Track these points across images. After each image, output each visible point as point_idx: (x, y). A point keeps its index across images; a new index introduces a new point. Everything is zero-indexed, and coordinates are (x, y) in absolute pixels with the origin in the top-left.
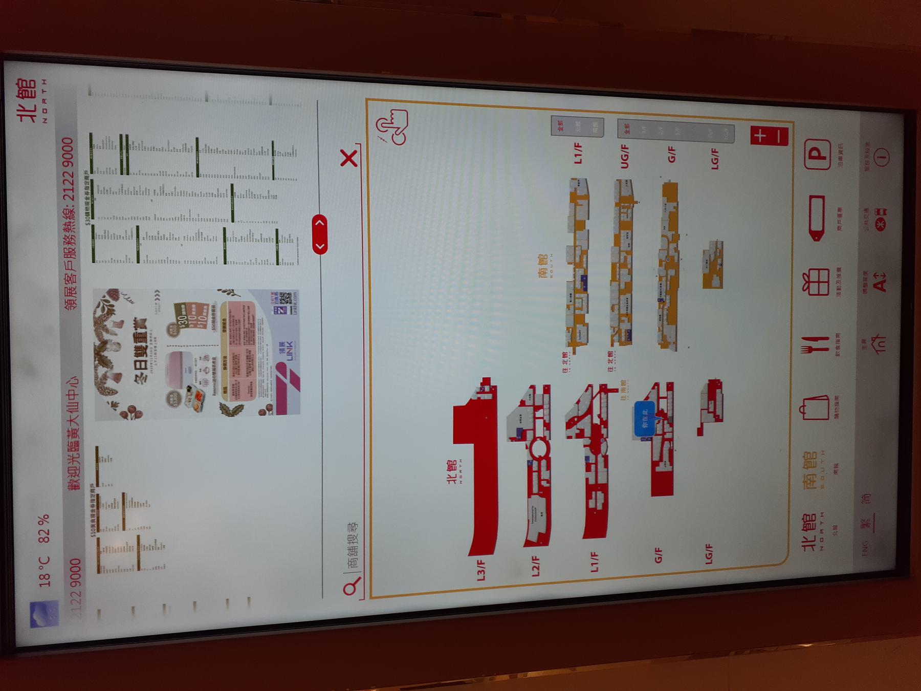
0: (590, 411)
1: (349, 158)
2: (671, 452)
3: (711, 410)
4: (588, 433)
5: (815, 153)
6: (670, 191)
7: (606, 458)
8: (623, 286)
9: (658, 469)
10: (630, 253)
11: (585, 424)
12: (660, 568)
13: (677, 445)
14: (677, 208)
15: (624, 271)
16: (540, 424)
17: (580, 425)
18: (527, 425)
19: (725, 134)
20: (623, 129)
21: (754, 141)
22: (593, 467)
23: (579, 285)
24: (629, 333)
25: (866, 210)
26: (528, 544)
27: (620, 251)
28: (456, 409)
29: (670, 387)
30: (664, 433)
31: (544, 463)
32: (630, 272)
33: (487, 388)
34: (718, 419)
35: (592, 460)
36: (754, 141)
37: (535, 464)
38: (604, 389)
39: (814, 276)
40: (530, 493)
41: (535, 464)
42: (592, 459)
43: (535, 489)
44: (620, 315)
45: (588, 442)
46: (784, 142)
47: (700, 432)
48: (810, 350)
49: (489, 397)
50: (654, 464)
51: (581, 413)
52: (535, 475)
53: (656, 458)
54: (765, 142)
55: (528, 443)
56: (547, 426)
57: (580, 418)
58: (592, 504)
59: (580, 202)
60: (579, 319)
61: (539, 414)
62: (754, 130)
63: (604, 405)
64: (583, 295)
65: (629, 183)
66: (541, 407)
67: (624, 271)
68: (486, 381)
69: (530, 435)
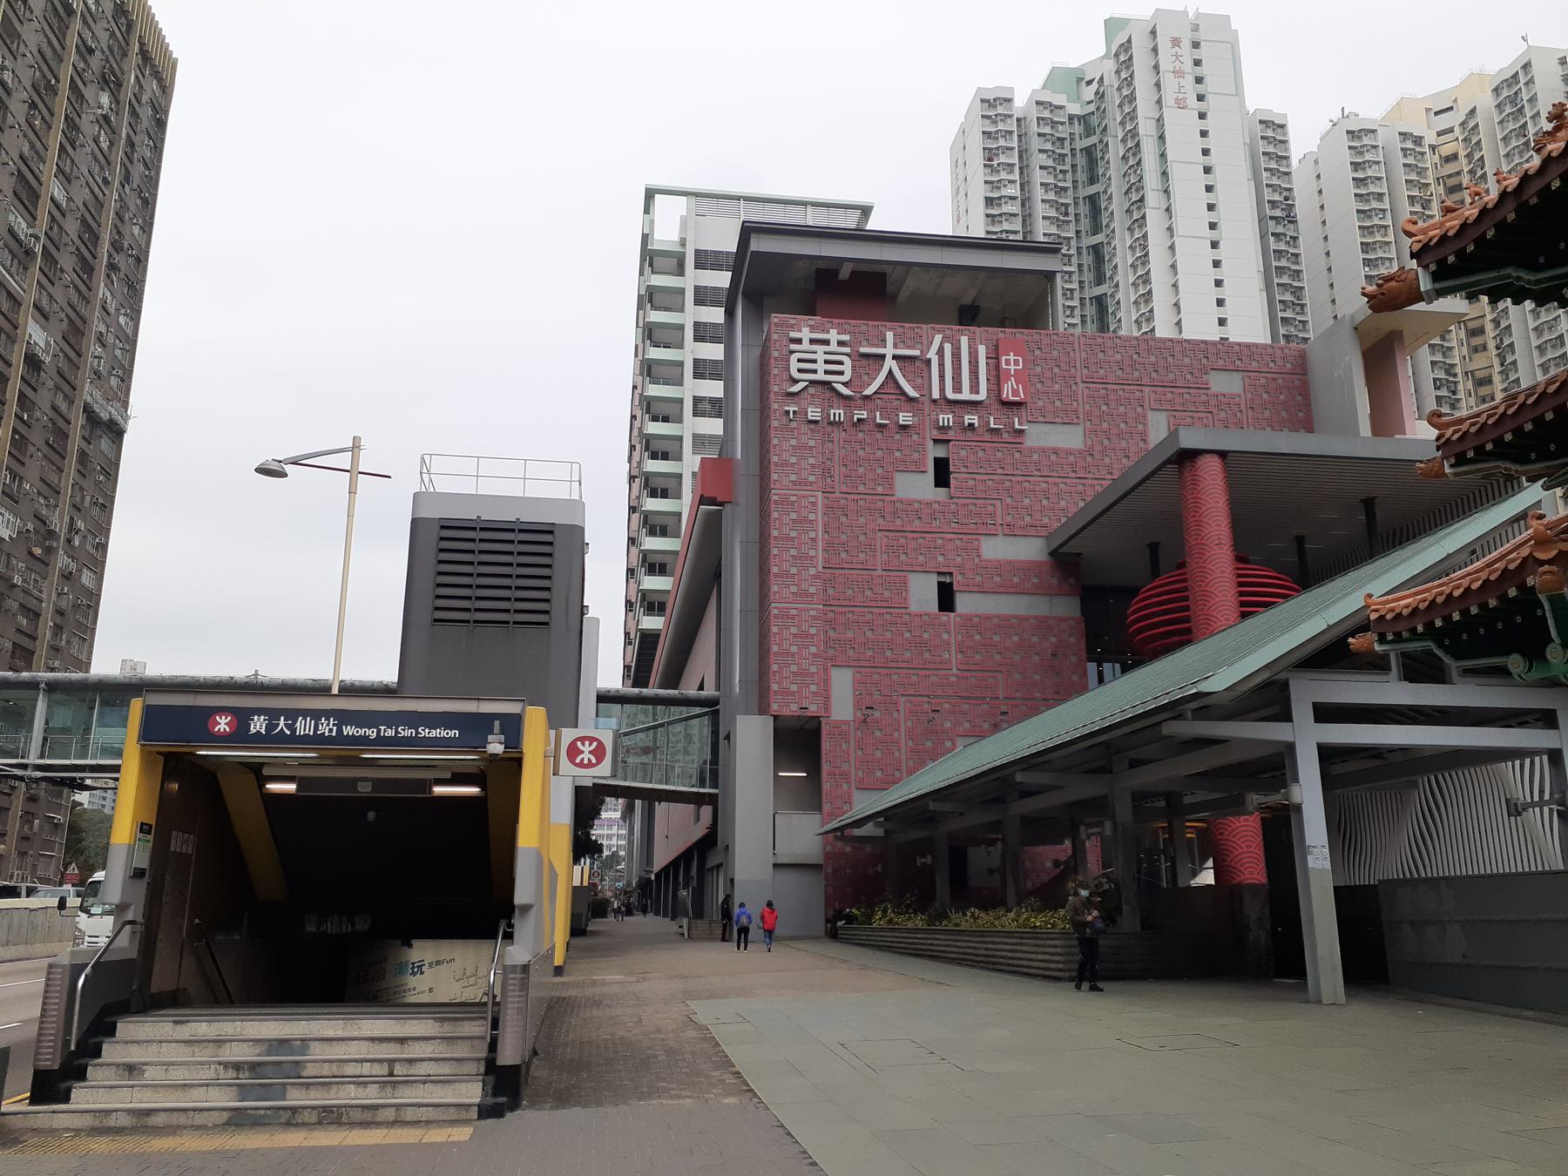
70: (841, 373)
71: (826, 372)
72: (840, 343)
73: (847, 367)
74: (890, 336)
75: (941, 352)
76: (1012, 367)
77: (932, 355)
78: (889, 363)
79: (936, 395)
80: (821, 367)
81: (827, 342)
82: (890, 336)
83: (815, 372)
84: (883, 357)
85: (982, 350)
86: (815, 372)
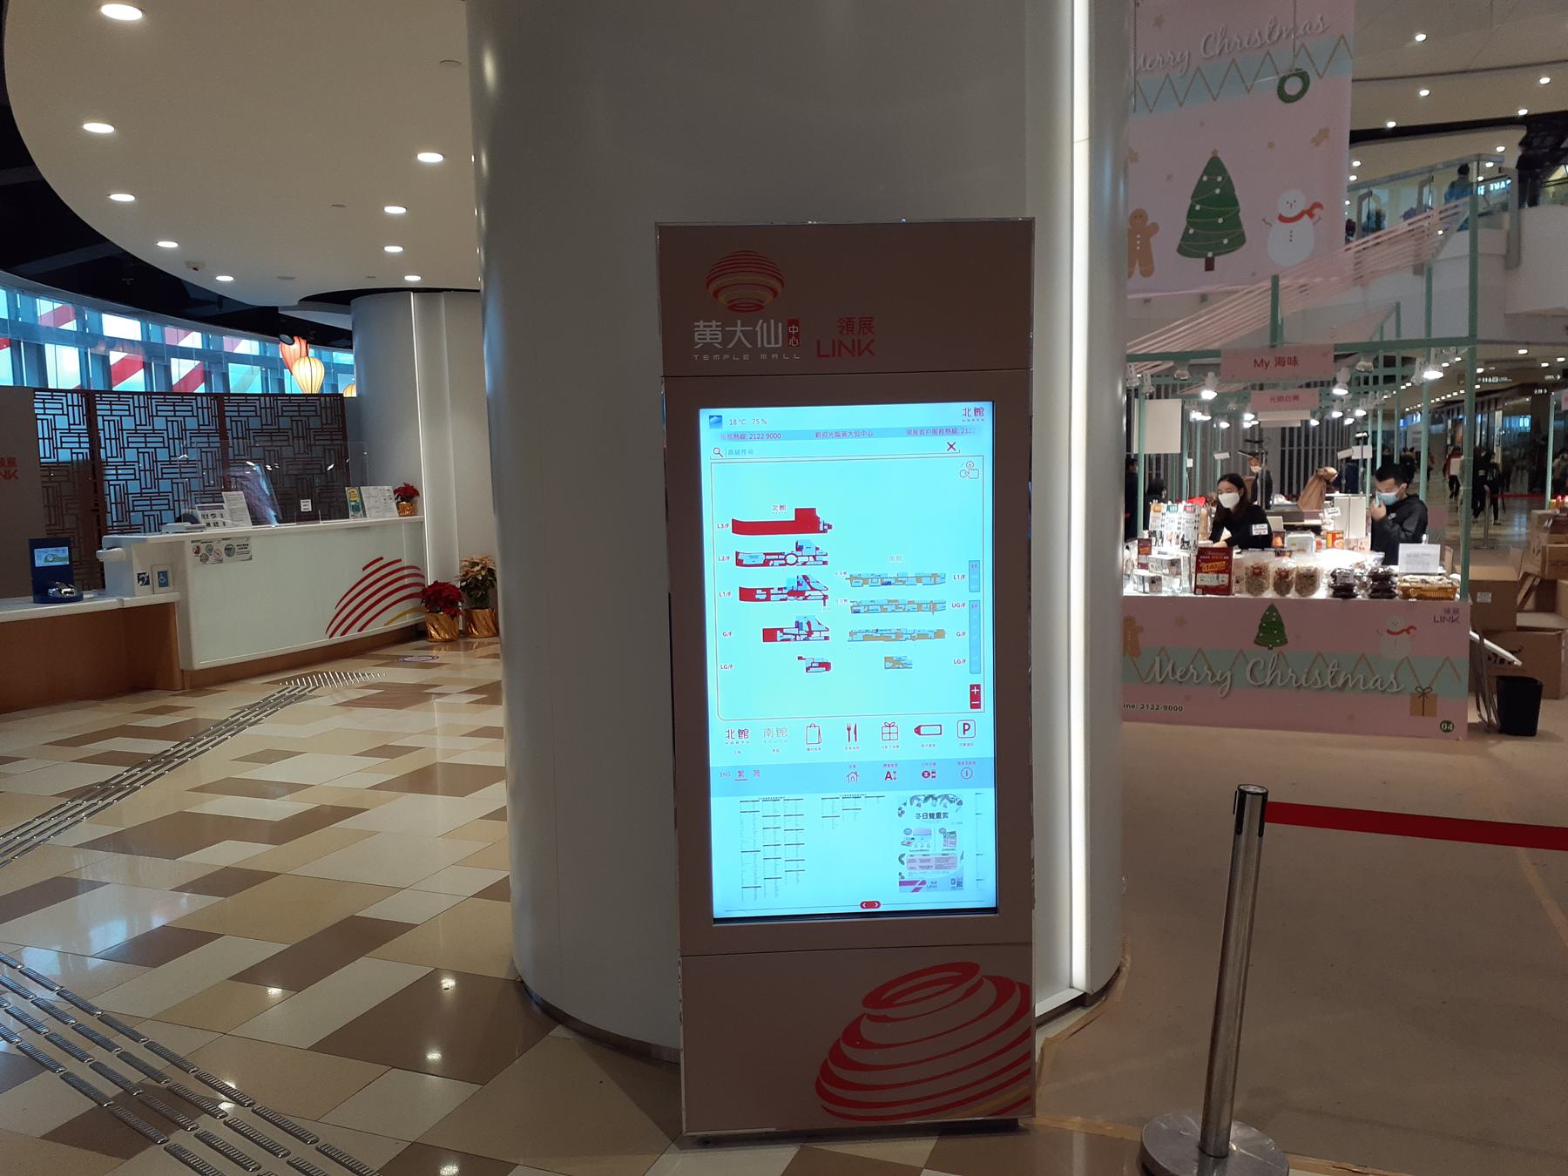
0: (813, 589)
1: (951, 446)
2: (789, 640)
3: (813, 665)
4: (800, 589)
5: (967, 727)
6: (940, 634)
7: (785, 600)
8: (885, 607)
9: (778, 632)
10: (904, 611)
11: (805, 587)
12: (720, 635)
13: (792, 643)
14: (931, 638)
15: (893, 608)
16: (806, 559)
17: (805, 584)
18: (805, 551)
19: (975, 668)
20: (974, 603)
21: (972, 687)
22: (780, 592)
23: (885, 580)
24: (858, 612)
25: (934, 764)
26: (737, 554)
27: (905, 604)
28: (813, 510)
29: (826, 638)
30: (799, 635)
31: (783, 562)
32: (893, 611)
33: (826, 527)
34: (807, 669)
35: (785, 591)
36: (972, 687)
37: (783, 557)
38: (825, 597)
39: (893, 730)
40: (766, 554)
41: (783, 557)
42: (785, 591)
43: (768, 557)
44: (868, 606)
45: (795, 589)
46: (973, 707)
47: (800, 658)
48: (849, 729)
49: (821, 529)
50: (781, 630)
51: (811, 584)
52: (776, 557)
53: (785, 631)
54: (972, 693)
55: (795, 552)
56: (804, 564)
57: (808, 583)
58: (758, 592)
59: (933, 579)
60: (865, 581)
61: (811, 558)
62: (978, 687)
63: (816, 598)
64: (879, 584)
65: (944, 609)
66: (815, 560)
67: (893, 608)
68: (830, 527)
69: (799, 553)
70: (717, 339)
71: (711, 339)
72: (717, 326)
73: (720, 336)
74: (739, 322)
75: (762, 328)
76: (794, 332)
77: (758, 329)
78: (739, 334)
79: (759, 345)
80: (708, 337)
81: (711, 326)
82: (739, 322)
83: (705, 339)
84: (736, 331)
85: (780, 324)
86: (705, 339)
